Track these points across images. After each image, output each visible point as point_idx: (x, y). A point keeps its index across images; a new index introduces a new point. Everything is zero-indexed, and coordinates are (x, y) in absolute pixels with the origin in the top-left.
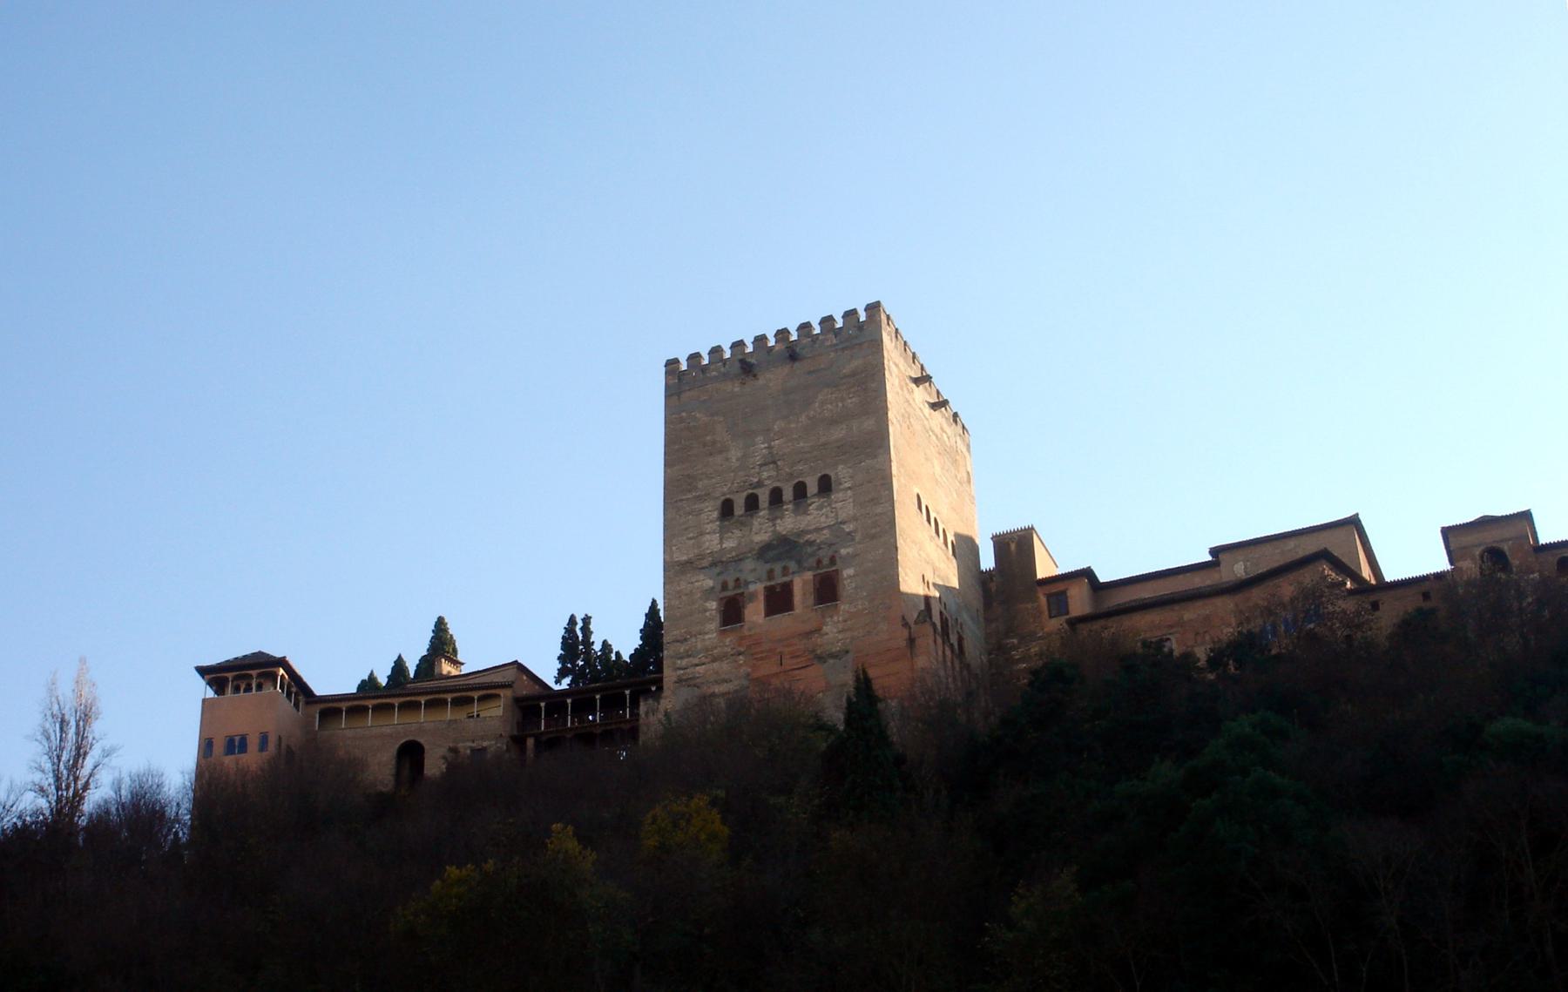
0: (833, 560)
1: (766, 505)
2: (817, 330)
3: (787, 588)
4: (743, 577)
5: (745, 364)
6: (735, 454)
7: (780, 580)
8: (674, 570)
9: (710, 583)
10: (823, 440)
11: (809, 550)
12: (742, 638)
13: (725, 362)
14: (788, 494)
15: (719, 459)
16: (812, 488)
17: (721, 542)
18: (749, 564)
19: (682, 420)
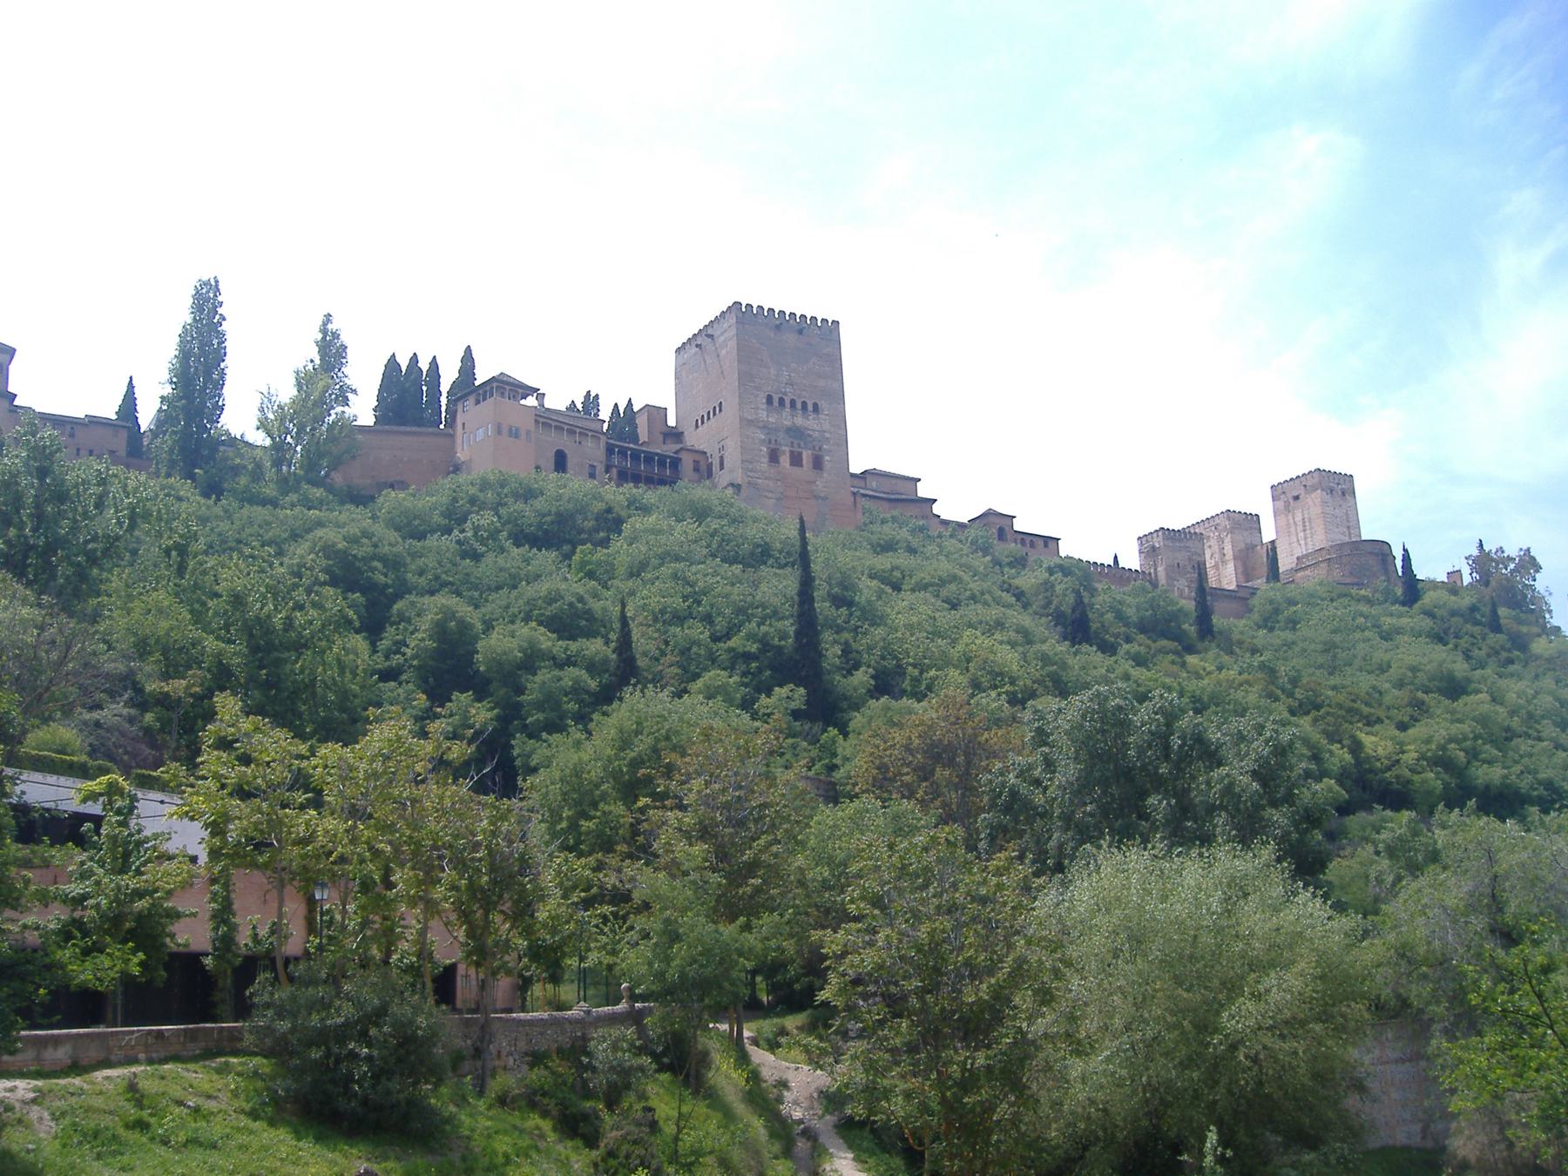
3: (800, 454)
6: (773, 372)
7: (797, 449)
14: (799, 405)
16: (810, 408)
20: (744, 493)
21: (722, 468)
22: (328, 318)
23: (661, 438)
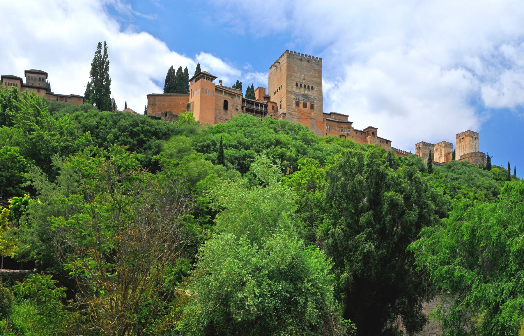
3: (306, 104)
6: (298, 75)
14: (307, 87)
16: (310, 88)
20: (287, 116)
21: (281, 108)
22: (172, 67)
23: (263, 98)
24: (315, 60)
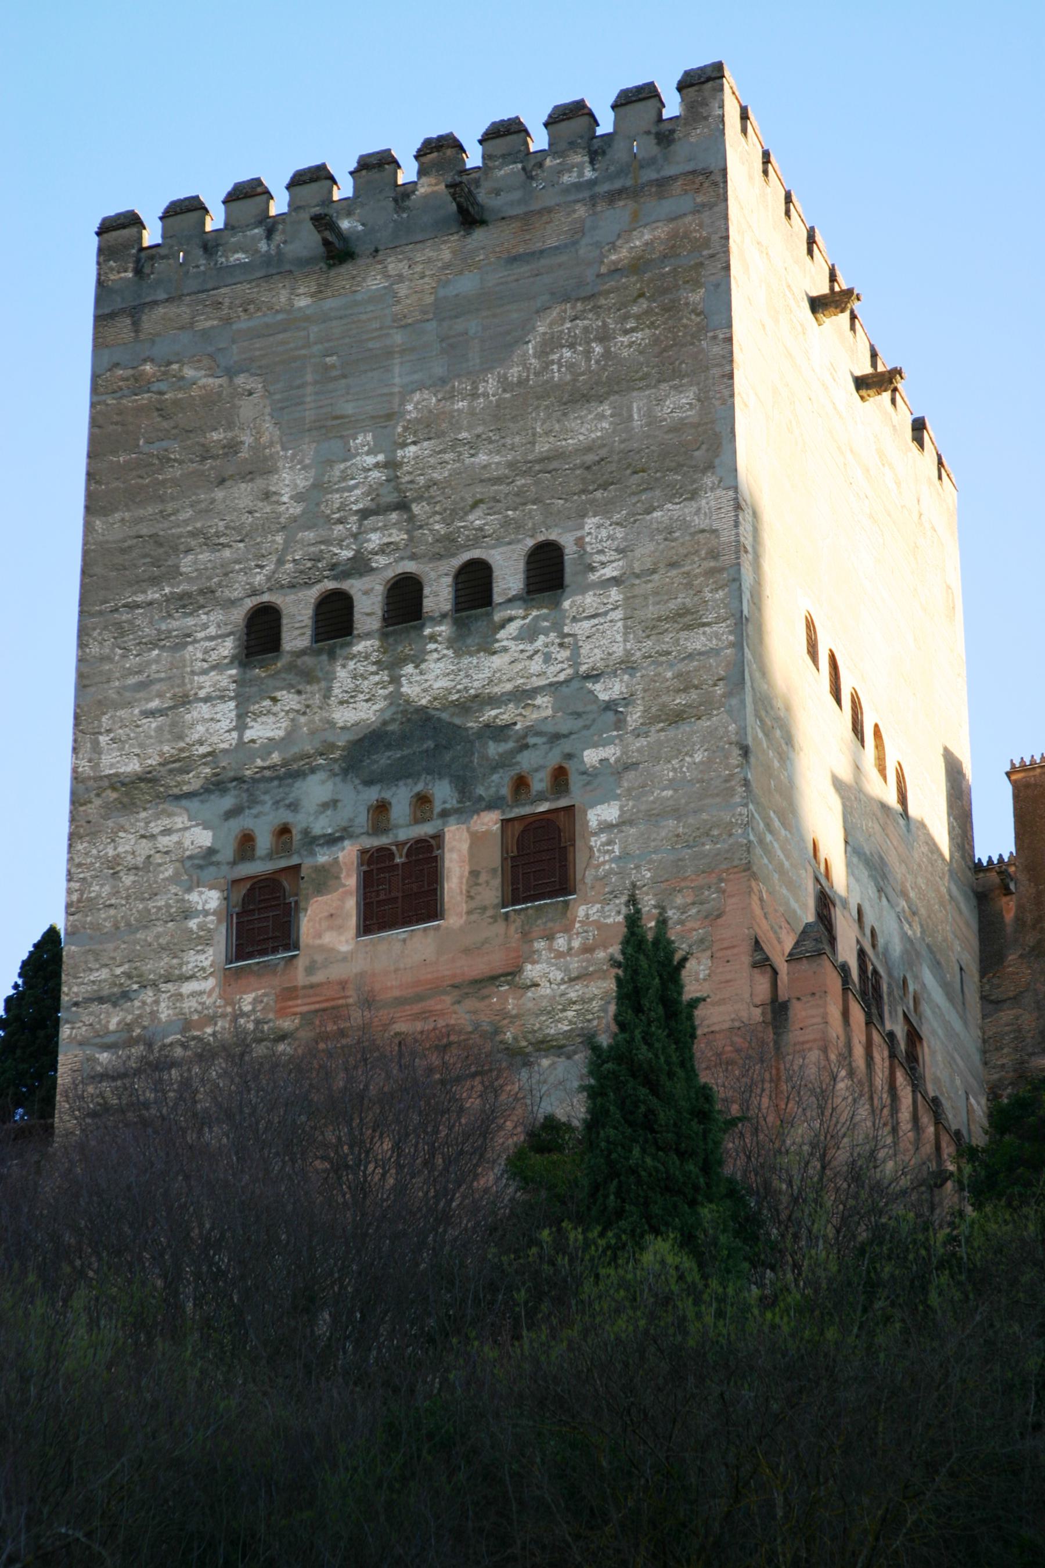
0: (560, 778)
1: (374, 623)
2: (539, 140)
3: (426, 856)
4: (298, 822)
5: (328, 229)
7: (406, 831)
8: (100, 801)
9: (204, 838)
10: (543, 447)
11: (494, 749)
12: (289, 993)
13: (271, 226)
14: (439, 594)
15: (243, 494)
16: (509, 576)
17: (241, 727)
18: (316, 789)
19: (139, 384)
24: (597, 149)
